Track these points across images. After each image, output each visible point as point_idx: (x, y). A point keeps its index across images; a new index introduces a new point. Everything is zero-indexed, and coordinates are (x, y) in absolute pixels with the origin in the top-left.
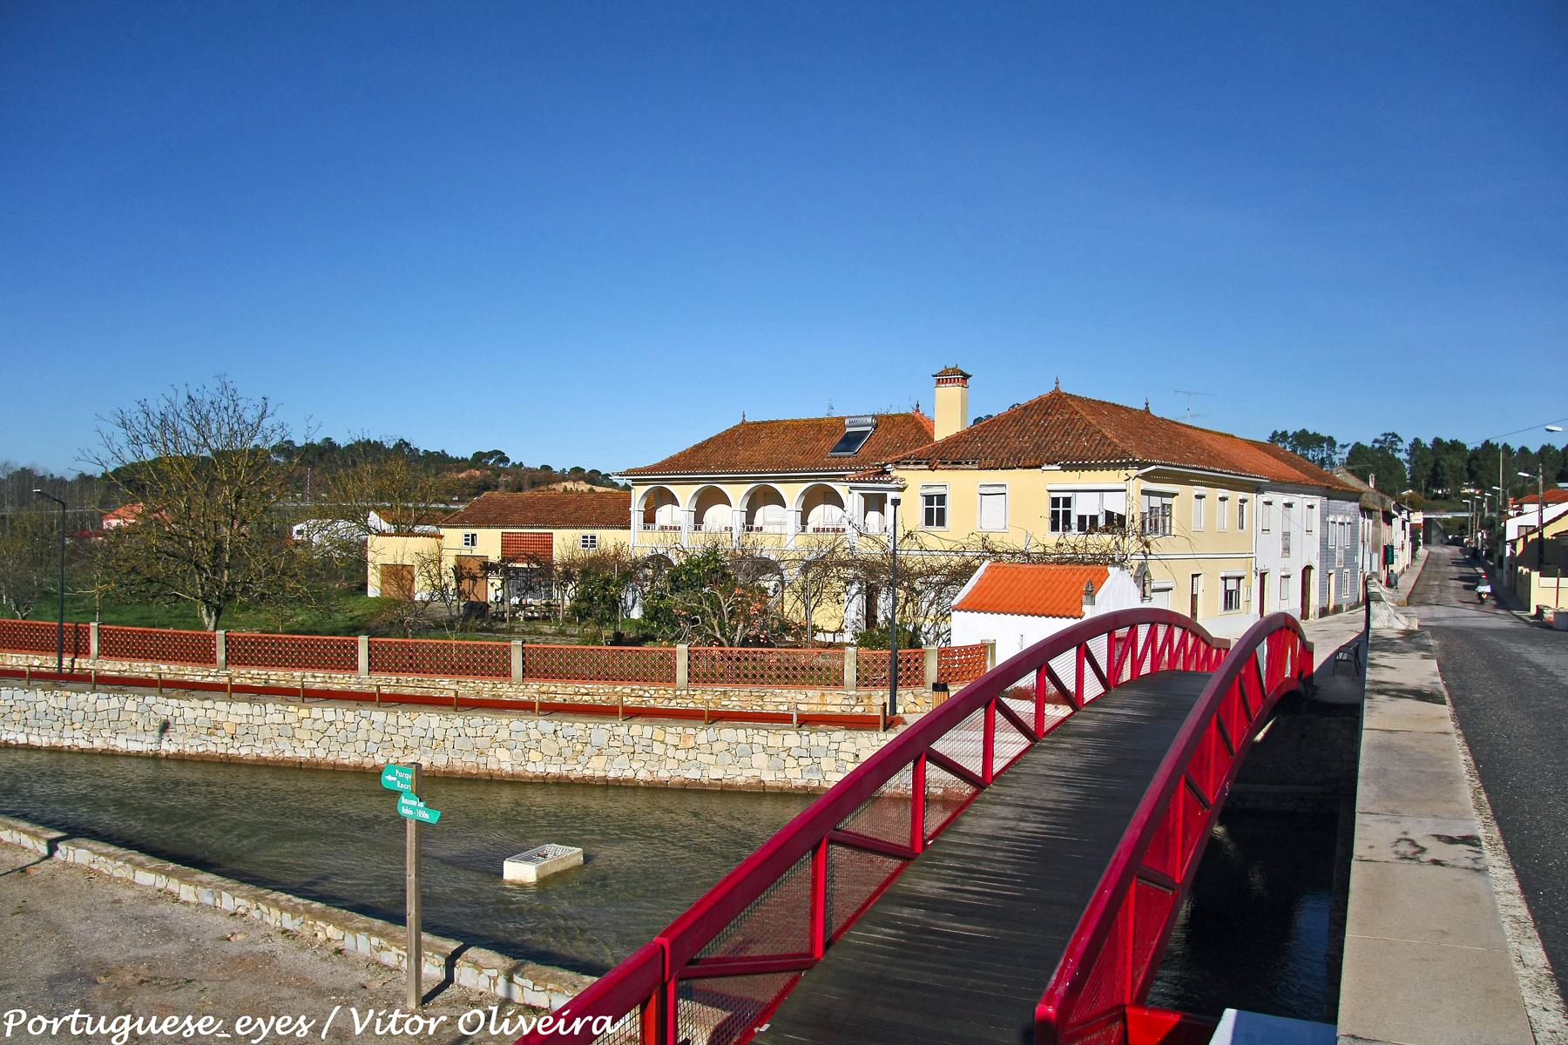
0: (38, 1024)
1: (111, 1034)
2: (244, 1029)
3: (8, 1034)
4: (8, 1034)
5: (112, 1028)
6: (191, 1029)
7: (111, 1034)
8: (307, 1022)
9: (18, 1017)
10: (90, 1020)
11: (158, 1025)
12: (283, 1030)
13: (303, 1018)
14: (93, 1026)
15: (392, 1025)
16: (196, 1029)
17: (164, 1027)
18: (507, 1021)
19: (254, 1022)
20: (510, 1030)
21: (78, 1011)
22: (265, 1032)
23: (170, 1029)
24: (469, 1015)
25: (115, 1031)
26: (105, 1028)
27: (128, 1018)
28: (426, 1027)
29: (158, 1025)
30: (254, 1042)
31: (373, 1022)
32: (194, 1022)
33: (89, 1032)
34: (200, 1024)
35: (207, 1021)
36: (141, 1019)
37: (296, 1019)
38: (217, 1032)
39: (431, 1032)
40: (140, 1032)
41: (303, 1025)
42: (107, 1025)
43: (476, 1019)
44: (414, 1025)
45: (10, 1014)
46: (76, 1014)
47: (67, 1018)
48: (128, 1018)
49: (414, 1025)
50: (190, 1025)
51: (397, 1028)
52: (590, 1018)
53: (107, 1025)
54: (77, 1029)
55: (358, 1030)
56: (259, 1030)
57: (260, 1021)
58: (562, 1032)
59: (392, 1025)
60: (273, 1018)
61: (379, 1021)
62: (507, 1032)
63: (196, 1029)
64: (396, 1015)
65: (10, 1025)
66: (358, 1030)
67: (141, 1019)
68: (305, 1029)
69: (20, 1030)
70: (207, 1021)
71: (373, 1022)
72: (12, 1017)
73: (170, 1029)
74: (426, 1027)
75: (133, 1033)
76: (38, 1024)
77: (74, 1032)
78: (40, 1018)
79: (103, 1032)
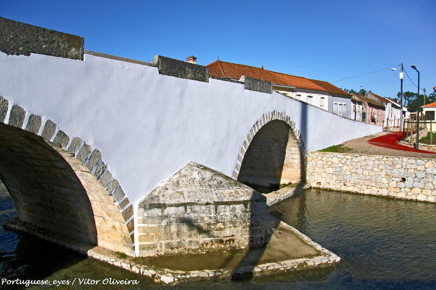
0: (9, 282)
1: (25, 284)
2: (55, 283)
3: (2, 284)
4: (2, 284)
5: (26, 283)
6: (43, 283)
7: (25, 284)
8: (69, 282)
9: (5, 280)
10: (21, 281)
11: (36, 282)
12: (64, 283)
13: (68, 281)
14: (21, 282)
15: (88, 282)
16: (44, 283)
17: (37, 283)
18: (113, 281)
19: (57, 281)
20: (137, 283)
21: (89, 279)
22: (60, 284)
23: (38, 283)
24: (105, 280)
25: (26, 283)
26: (24, 283)
27: (29, 281)
28: (12, 282)
29: (36, 282)
30: (57, 286)
31: (83, 282)
32: (44, 282)
33: (20, 284)
34: (45, 282)
35: (47, 281)
36: (32, 281)
37: (66, 281)
38: (49, 284)
39: (13, 284)
40: (32, 284)
41: (68, 282)
42: (24, 282)
43: (106, 280)
44: (93, 282)
45: (3, 280)
46: (18, 280)
47: (15, 281)
48: (29, 281)
49: (93, 282)
50: (43, 282)
51: (89, 283)
52: (132, 281)
53: (24, 282)
54: (18, 283)
55: (80, 283)
56: (58, 283)
57: (58, 281)
58: (126, 284)
59: (88, 282)
60: (61, 281)
61: (85, 281)
62: (136, 283)
63: (44, 283)
64: (89, 280)
65: (3, 282)
66: (80, 283)
67: (32, 281)
68: (68, 283)
69: (5, 283)
70: (47, 281)
71: (83, 282)
72: (3, 280)
73: (38, 283)
74: (95, 282)
75: (30, 284)
76: (9, 282)
77: (17, 284)
78: (10, 280)
79: (24, 284)
